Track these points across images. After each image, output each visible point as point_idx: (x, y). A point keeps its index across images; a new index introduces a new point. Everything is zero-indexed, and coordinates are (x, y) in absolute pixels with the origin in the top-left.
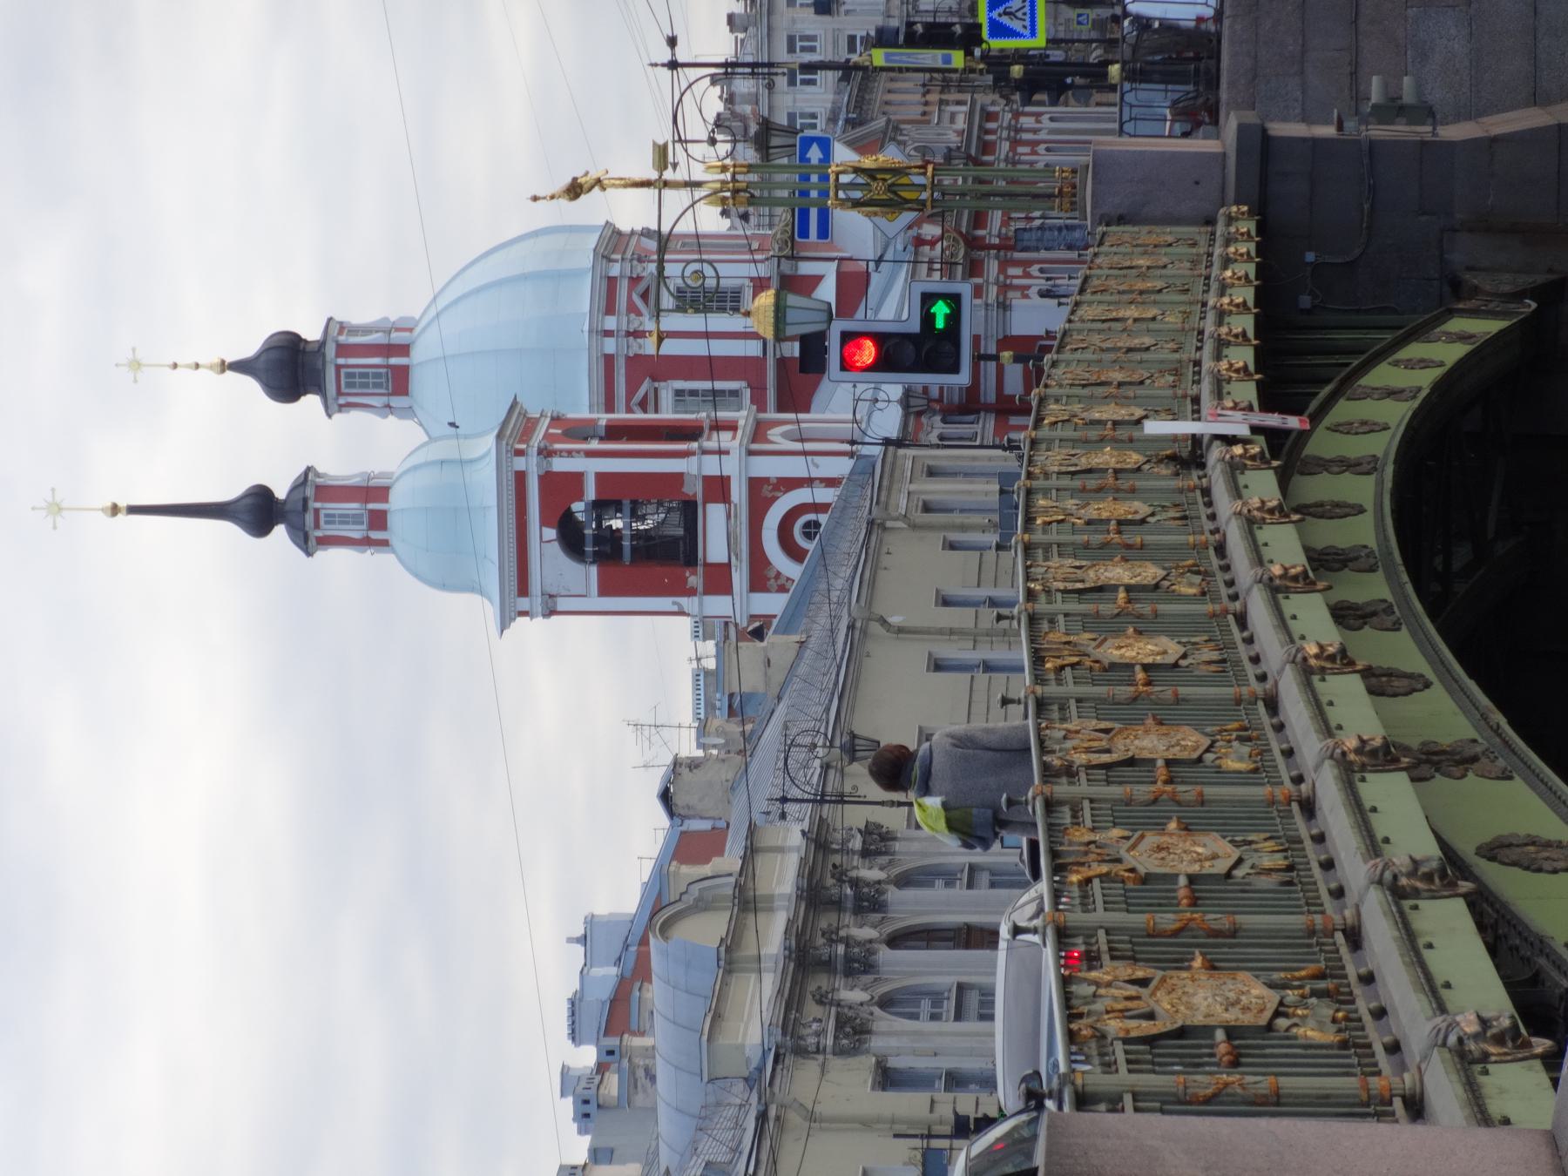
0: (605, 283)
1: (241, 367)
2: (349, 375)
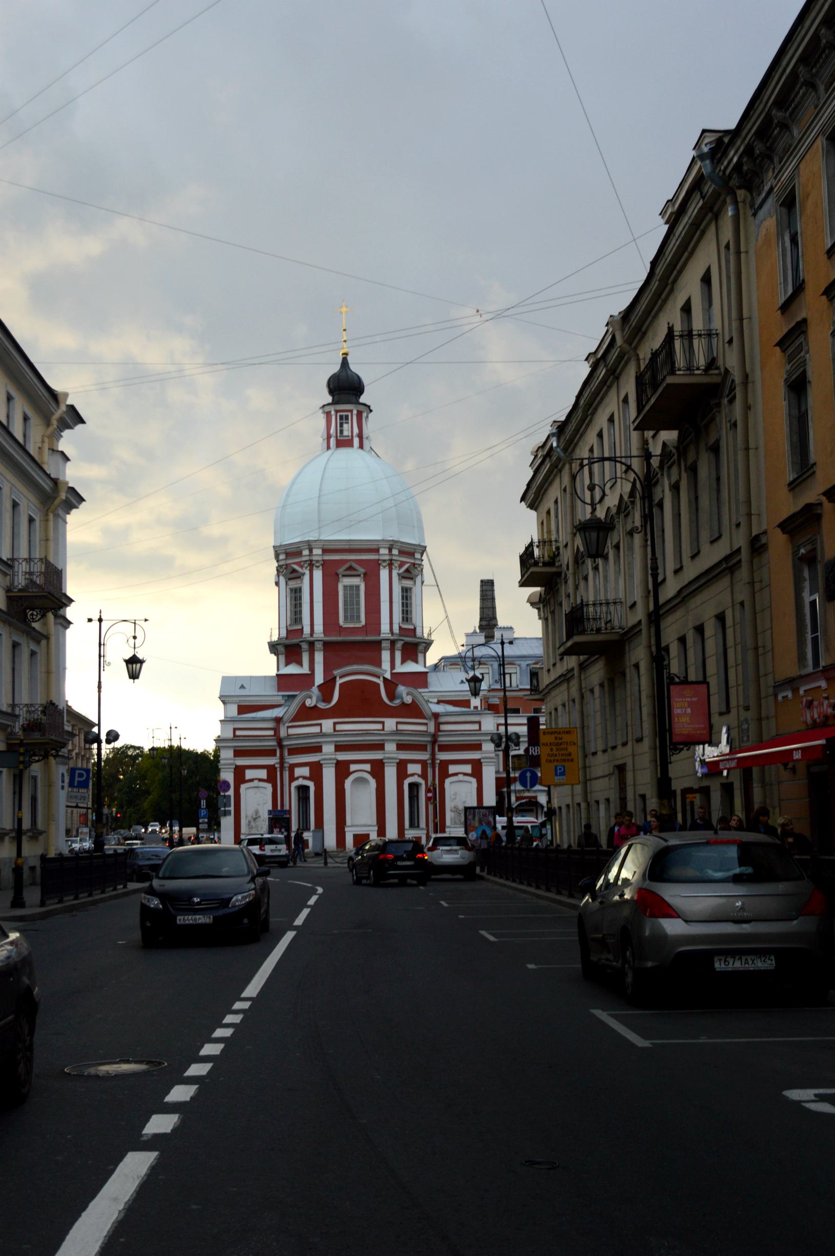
0: (412, 551)
1: (345, 363)
2: (347, 417)
